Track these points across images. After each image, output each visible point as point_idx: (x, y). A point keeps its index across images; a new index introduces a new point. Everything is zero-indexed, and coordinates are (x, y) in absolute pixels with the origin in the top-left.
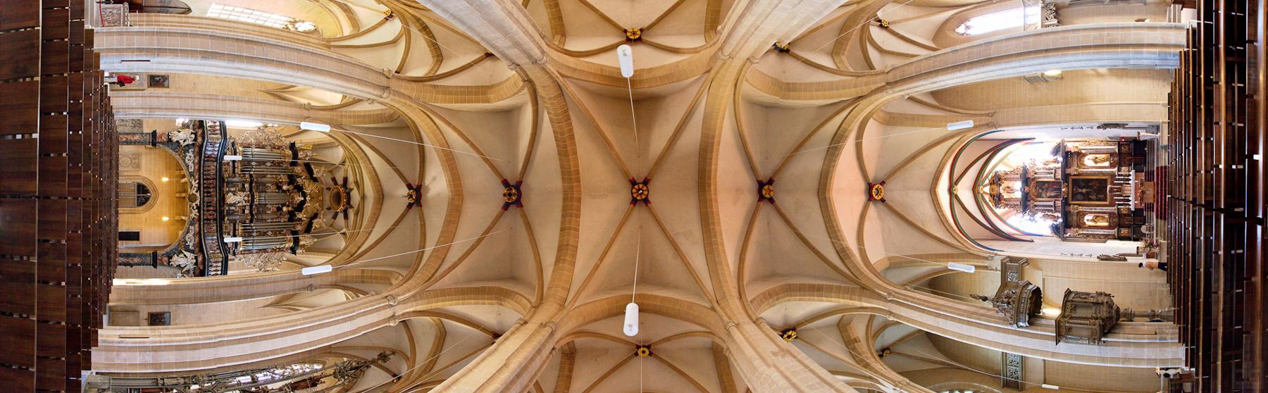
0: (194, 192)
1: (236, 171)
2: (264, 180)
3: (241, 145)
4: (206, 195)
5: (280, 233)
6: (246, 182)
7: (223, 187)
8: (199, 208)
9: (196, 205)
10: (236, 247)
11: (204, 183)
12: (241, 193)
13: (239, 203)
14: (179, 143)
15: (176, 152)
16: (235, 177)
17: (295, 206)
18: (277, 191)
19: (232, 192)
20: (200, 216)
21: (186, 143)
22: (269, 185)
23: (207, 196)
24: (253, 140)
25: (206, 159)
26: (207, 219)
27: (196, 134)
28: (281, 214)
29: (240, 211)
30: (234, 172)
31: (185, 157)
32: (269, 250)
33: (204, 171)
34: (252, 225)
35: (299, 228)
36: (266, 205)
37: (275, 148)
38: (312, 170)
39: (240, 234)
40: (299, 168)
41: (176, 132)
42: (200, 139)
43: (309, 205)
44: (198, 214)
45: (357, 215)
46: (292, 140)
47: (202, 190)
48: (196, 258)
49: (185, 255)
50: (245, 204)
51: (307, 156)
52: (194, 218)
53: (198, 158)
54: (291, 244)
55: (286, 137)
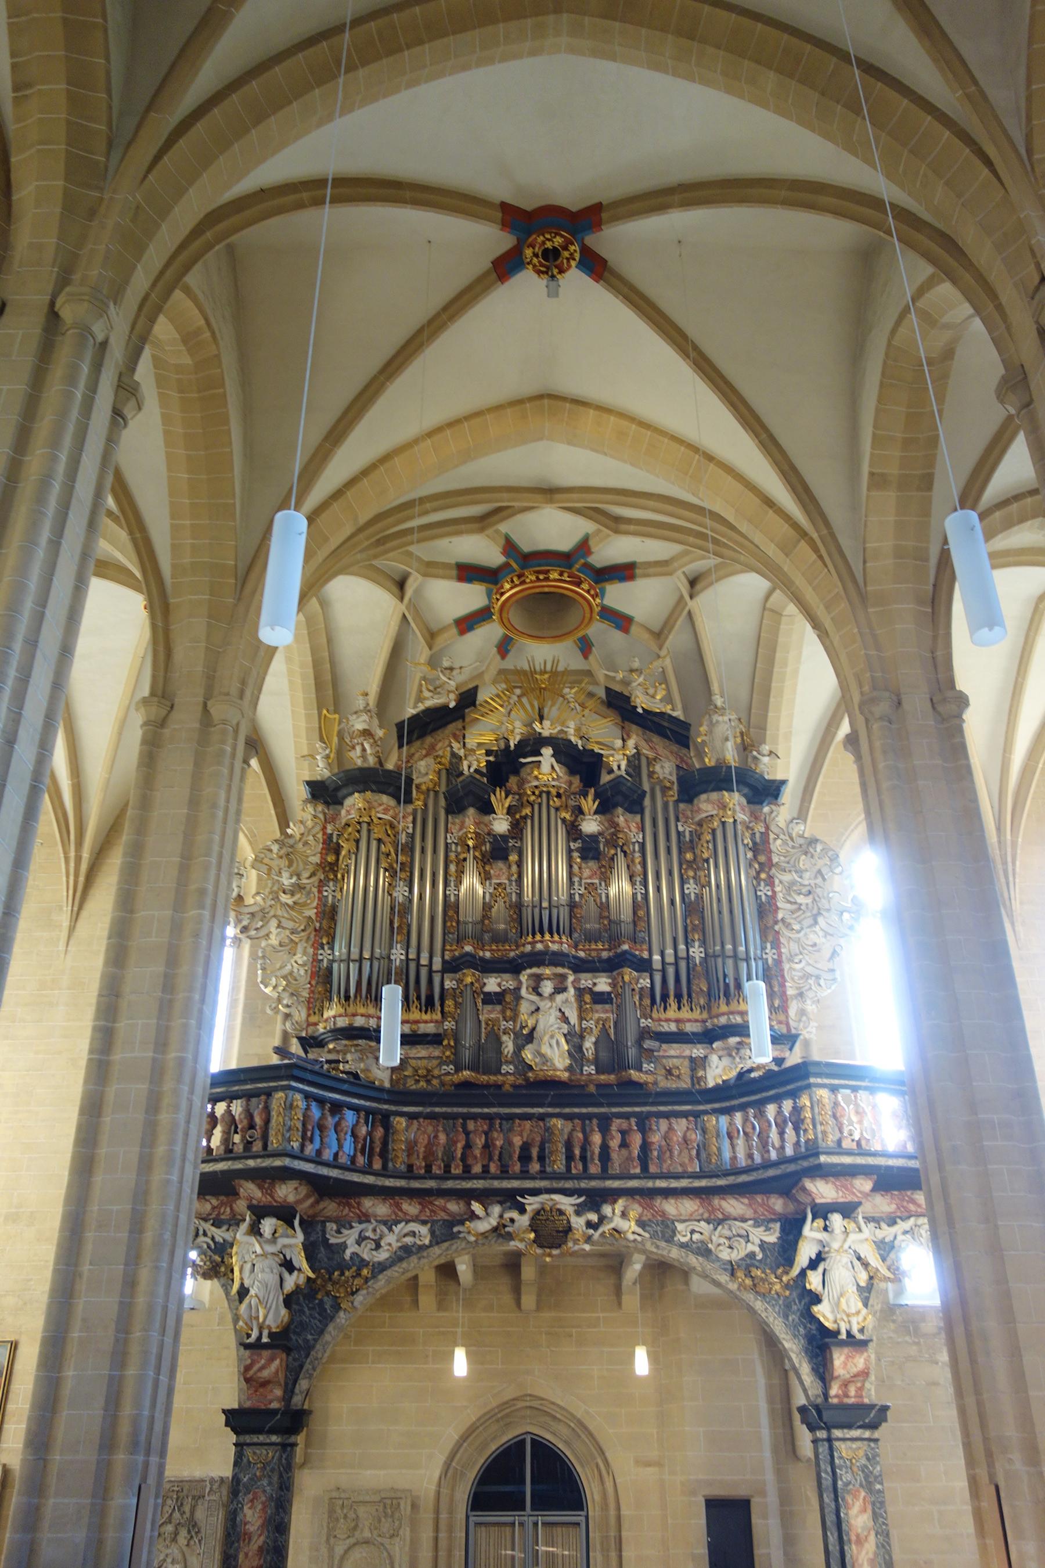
0: (524, 1220)
1: (430, 1028)
2: (470, 914)
3: (315, 1006)
4: (535, 1167)
5: (692, 849)
7: (499, 1086)
8: (595, 1200)
9: (578, 1213)
12: (524, 1008)
13: (565, 1019)
15: (337, 1307)
16: (456, 1035)
17: (576, 781)
18: (513, 857)
19: (519, 1049)
20: (630, 1193)
21: (300, 1260)
23: (541, 1158)
24: (299, 962)
25: (377, 1165)
26: (644, 1158)
27: (260, 1212)
28: (612, 843)
29: (602, 1013)
30: (435, 1040)
31: (364, 1263)
32: (764, 891)
33: (429, 1174)
35: (666, 769)
36: (572, 905)
37: (333, 867)
38: (428, 711)
39: (696, 1014)
40: (422, 766)
43: (572, 724)
45: (618, 519)
46: (297, 793)
51: (367, 733)
52: (641, 1223)
54: (735, 799)
55: (284, 820)
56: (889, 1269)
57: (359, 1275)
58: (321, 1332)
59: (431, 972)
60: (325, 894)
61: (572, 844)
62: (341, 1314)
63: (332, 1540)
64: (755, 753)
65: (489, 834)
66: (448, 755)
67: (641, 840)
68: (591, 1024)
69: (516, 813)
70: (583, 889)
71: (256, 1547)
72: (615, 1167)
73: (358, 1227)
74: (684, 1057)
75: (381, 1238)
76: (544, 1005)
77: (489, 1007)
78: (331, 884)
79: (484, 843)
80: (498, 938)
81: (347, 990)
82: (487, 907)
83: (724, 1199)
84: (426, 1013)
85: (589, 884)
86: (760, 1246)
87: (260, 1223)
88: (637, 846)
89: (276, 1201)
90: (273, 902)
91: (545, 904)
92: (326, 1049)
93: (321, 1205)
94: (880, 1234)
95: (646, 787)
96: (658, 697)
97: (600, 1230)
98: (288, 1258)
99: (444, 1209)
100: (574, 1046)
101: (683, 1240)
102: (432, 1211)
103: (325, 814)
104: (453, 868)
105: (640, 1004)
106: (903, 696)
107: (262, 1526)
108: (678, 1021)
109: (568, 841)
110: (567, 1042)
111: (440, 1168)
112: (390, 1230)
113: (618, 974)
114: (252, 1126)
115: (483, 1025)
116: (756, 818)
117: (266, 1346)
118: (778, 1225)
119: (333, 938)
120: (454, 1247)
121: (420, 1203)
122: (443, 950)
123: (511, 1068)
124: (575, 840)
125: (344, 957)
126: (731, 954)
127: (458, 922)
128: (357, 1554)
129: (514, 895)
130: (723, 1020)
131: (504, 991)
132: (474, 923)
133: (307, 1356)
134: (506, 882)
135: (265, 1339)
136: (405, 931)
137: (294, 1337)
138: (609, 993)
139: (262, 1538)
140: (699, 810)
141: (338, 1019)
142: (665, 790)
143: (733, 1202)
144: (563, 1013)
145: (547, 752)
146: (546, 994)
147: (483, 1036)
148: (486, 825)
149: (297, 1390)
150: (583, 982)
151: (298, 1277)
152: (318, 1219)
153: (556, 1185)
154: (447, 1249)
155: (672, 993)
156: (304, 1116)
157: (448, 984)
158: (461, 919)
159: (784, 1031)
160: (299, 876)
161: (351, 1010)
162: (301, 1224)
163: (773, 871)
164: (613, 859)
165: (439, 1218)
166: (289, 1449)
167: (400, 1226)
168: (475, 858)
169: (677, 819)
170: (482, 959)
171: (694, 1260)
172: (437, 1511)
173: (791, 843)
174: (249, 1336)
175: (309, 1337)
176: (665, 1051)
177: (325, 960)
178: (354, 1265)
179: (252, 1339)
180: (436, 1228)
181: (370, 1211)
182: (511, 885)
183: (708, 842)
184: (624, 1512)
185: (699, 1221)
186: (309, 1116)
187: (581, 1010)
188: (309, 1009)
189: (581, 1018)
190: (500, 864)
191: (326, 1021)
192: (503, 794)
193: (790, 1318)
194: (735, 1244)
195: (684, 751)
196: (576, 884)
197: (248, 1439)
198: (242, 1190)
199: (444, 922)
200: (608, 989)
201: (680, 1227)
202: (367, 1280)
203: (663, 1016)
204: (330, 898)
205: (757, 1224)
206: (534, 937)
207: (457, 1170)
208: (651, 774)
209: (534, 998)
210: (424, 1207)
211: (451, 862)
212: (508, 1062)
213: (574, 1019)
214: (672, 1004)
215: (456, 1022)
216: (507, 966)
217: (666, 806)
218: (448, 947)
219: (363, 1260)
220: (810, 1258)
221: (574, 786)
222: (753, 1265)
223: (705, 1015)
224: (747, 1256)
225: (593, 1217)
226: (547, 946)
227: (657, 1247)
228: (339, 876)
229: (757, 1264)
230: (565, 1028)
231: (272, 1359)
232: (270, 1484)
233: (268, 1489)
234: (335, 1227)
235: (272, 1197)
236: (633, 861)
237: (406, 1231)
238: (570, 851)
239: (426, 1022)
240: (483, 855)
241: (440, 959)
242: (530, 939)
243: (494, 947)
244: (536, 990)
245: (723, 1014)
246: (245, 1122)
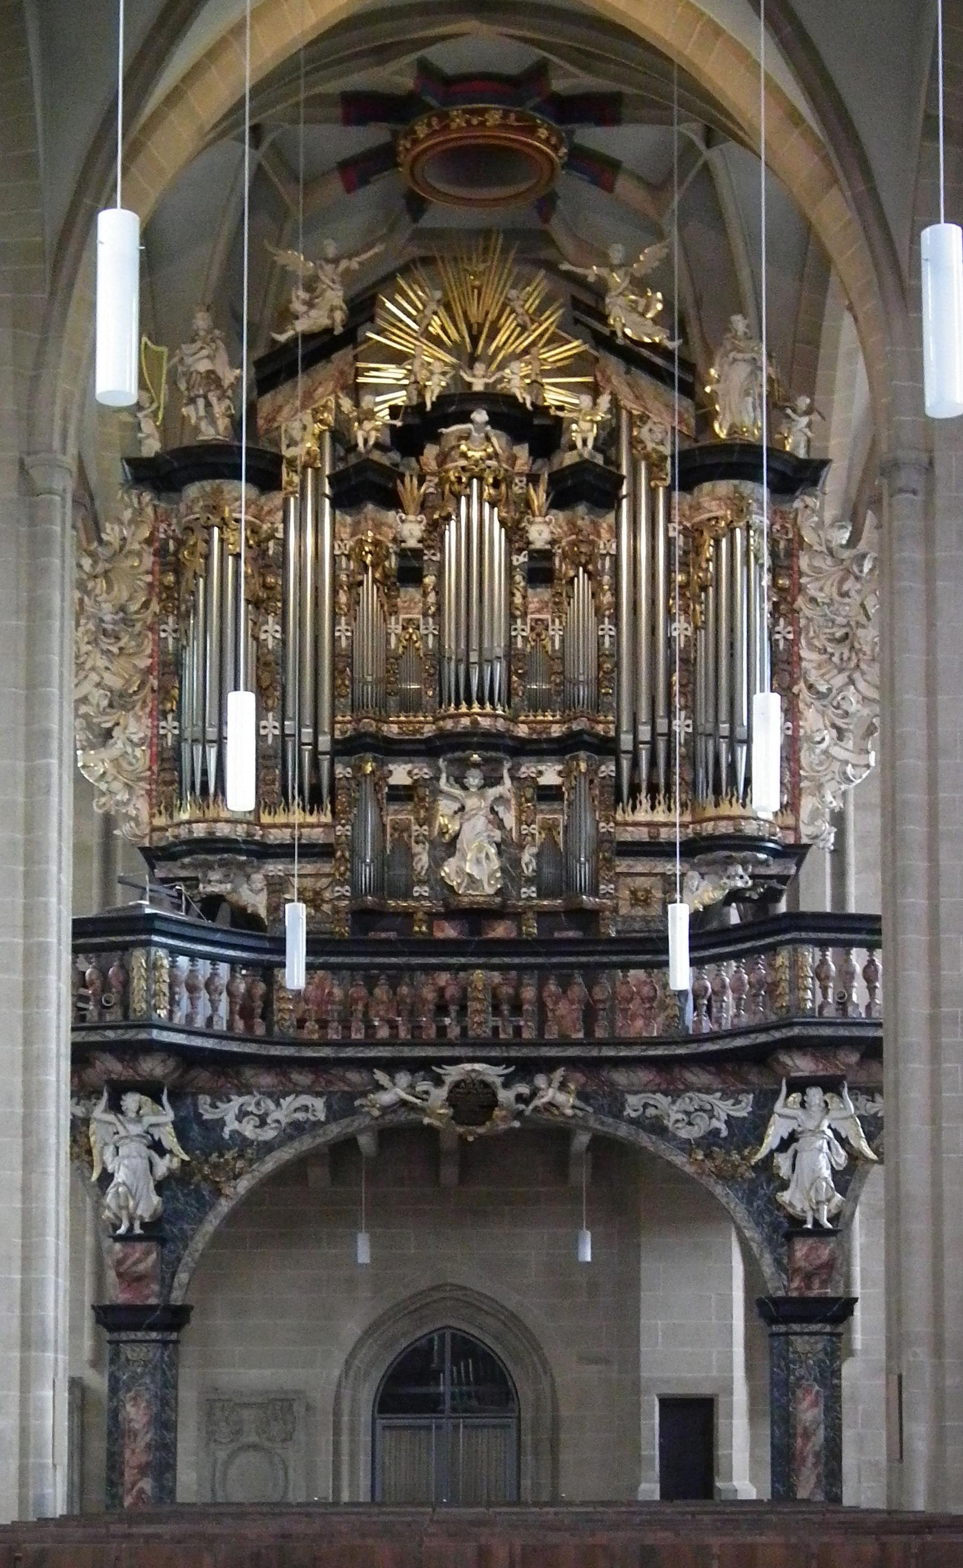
0: (439, 1095)
6: (380, 777)
7: (408, 915)
9: (506, 1085)
10: (753, 843)
11: (392, 1041)
14: (171, 1175)
16: (353, 845)
17: (522, 452)
18: (429, 580)
20: (571, 1063)
21: (170, 1140)
22: (395, 626)
23: (463, 1009)
26: (589, 1015)
29: (547, 813)
34: (626, 741)
36: (511, 656)
41: (109, 1199)
42: (153, 1067)
44: (559, 1074)
48: (799, 1085)
49: (785, 1144)
50: (506, 787)
52: (582, 1095)
53: (248, 1073)
56: (876, 1152)
57: (241, 1156)
58: (201, 1221)
59: (315, 753)
60: (163, 635)
61: (514, 558)
62: (223, 1201)
63: (212, 1445)
64: (789, 411)
65: (394, 540)
66: (332, 405)
67: (613, 552)
69: (434, 508)
70: (528, 629)
71: (143, 1444)
72: (552, 1033)
73: (237, 1101)
74: (656, 875)
75: (266, 1114)
76: (471, 803)
78: (171, 620)
79: (387, 557)
80: (410, 704)
81: (205, 785)
82: (392, 659)
84: (311, 813)
85: (537, 620)
86: (726, 1122)
87: (121, 1099)
88: (608, 558)
90: (89, 647)
91: (474, 657)
92: (178, 863)
93: (193, 1073)
94: (871, 1108)
95: (624, 471)
96: (649, 315)
97: (531, 1107)
98: (156, 1138)
99: (343, 1080)
100: (509, 859)
101: (633, 1115)
103: (155, 507)
104: (343, 598)
105: (600, 802)
106: (937, 454)
107: (149, 1423)
108: (648, 824)
109: (509, 554)
110: (500, 853)
111: (337, 1033)
112: (278, 1105)
113: (572, 758)
114: (106, 986)
115: (389, 830)
116: (783, 516)
117: (139, 1238)
118: (751, 1096)
119: (179, 703)
120: (356, 1124)
121: (312, 1073)
122: (333, 723)
123: (425, 890)
124: (519, 551)
125: (199, 735)
126: (726, 733)
127: (352, 680)
128: (243, 1459)
129: (431, 637)
130: (709, 828)
131: (416, 781)
132: (377, 682)
133: (186, 1247)
135: (138, 1230)
136: (278, 694)
137: (167, 1227)
138: (559, 787)
139: (149, 1436)
140: (697, 507)
141: (194, 825)
142: (655, 466)
143: (696, 1070)
144: (497, 813)
146: (473, 790)
147: (389, 846)
148: (391, 527)
149: (176, 1284)
150: (523, 769)
151: (171, 1161)
152: (189, 1090)
153: (479, 1054)
154: (348, 1126)
155: (644, 786)
156: (170, 977)
157: (340, 771)
158: (356, 676)
159: (791, 840)
160: (122, 609)
161: (211, 814)
162: (169, 1100)
163: (800, 602)
164: (571, 582)
166: (171, 1346)
167: (289, 1099)
168: (375, 581)
169: (668, 519)
170: (388, 740)
171: (646, 1140)
172: (337, 1414)
173: (829, 561)
174: (116, 1227)
175: (186, 1226)
177: (170, 736)
178: (236, 1145)
179: (122, 1230)
180: (334, 1100)
182: (426, 623)
183: (708, 560)
184: (564, 1412)
185: (654, 1092)
186: (176, 976)
187: (520, 812)
188: (151, 806)
190: (411, 590)
191: (179, 825)
192: (415, 481)
193: (755, 1204)
194: (698, 1120)
195: (687, 402)
196: (519, 621)
197: (124, 1336)
199: (333, 679)
200: (556, 780)
201: (632, 1100)
202: (251, 1162)
203: (630, 818)
204: (170, 641)
205: (725, 1096)
206: (457, 706)
207: (357, 1035)
208: (634, 442)
209: (457, 792)
210: (318, 1077)
211: (342, 588)
212: (421, 883)
213: (510, 820)
214: (644, 801)
215: (353, 826)
216: (423, 747)
217: (652, 493)
218: (339, 718)
219: (245, 1139)
220: (782, 1139)
221: (519, 462)
222: (715, 1144)
223: (688, 818)
224: (710, 1133)
225: (524, 1089)
226: (475, 723)
227: (602, 1123)
228: (183, 608)
230: (497, 835)
231: (147, 1253)
232: (153, 1382)
233: (152, 1386)
236: (600, 584)
238: (510, 569)
239: (312, 826)
240: (386, 576)
241: (329, 737)
242: (452, 710)
243: (402, 719)
244: (460, 782)
245: (710, 819)
246: (98, 983)
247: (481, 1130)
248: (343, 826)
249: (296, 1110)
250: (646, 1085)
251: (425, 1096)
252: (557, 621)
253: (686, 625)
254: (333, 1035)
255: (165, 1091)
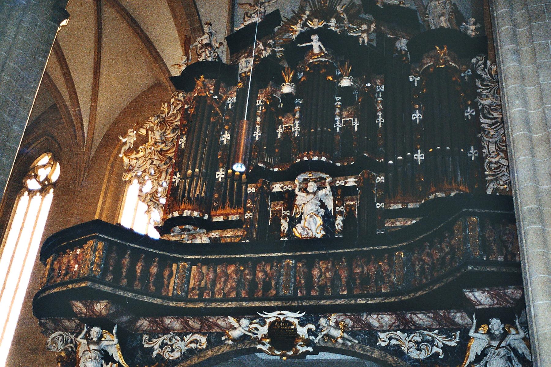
0: (264, 330)
1: (235, 217)
9: (302, 325)
13: (323, 205)
47: (257, 304)
68: (342, 209)
77: (276, 203)
83: (415, 314)
86: (442, 348)
89: (95, 315)
99: (216, 325)
101: (383, 344)
102: (208, 326)
111: (209, 295)
118: (458, 333)
120: (222, 350)
134: (292, 125)
145: (315, 38)
165: (214, 331)
167: (188, 337)
176: (393, 223)
181: (169, 326)
185: (396, 331)
189: (335, 206)
198: (74, 308)
201: (382, 335)
220: (477, 354)
227: (364, 350)
229: (440, 362)
230: (322, 212)
234: (148, 338)
235: (93, 312)
237: (191, 339)
244: (305, 190)
247: (291, 353)
248: (249, 213)
249: (191, 343)
250: (391, 326)
251: (256, 332)
252: (356, 120)
253: (419, 115)
254: (206, 296)
255: (116, 327)
